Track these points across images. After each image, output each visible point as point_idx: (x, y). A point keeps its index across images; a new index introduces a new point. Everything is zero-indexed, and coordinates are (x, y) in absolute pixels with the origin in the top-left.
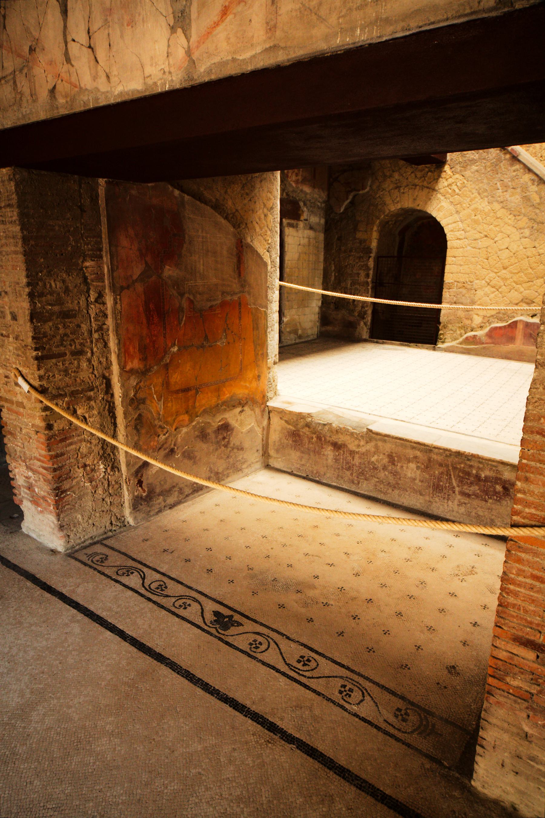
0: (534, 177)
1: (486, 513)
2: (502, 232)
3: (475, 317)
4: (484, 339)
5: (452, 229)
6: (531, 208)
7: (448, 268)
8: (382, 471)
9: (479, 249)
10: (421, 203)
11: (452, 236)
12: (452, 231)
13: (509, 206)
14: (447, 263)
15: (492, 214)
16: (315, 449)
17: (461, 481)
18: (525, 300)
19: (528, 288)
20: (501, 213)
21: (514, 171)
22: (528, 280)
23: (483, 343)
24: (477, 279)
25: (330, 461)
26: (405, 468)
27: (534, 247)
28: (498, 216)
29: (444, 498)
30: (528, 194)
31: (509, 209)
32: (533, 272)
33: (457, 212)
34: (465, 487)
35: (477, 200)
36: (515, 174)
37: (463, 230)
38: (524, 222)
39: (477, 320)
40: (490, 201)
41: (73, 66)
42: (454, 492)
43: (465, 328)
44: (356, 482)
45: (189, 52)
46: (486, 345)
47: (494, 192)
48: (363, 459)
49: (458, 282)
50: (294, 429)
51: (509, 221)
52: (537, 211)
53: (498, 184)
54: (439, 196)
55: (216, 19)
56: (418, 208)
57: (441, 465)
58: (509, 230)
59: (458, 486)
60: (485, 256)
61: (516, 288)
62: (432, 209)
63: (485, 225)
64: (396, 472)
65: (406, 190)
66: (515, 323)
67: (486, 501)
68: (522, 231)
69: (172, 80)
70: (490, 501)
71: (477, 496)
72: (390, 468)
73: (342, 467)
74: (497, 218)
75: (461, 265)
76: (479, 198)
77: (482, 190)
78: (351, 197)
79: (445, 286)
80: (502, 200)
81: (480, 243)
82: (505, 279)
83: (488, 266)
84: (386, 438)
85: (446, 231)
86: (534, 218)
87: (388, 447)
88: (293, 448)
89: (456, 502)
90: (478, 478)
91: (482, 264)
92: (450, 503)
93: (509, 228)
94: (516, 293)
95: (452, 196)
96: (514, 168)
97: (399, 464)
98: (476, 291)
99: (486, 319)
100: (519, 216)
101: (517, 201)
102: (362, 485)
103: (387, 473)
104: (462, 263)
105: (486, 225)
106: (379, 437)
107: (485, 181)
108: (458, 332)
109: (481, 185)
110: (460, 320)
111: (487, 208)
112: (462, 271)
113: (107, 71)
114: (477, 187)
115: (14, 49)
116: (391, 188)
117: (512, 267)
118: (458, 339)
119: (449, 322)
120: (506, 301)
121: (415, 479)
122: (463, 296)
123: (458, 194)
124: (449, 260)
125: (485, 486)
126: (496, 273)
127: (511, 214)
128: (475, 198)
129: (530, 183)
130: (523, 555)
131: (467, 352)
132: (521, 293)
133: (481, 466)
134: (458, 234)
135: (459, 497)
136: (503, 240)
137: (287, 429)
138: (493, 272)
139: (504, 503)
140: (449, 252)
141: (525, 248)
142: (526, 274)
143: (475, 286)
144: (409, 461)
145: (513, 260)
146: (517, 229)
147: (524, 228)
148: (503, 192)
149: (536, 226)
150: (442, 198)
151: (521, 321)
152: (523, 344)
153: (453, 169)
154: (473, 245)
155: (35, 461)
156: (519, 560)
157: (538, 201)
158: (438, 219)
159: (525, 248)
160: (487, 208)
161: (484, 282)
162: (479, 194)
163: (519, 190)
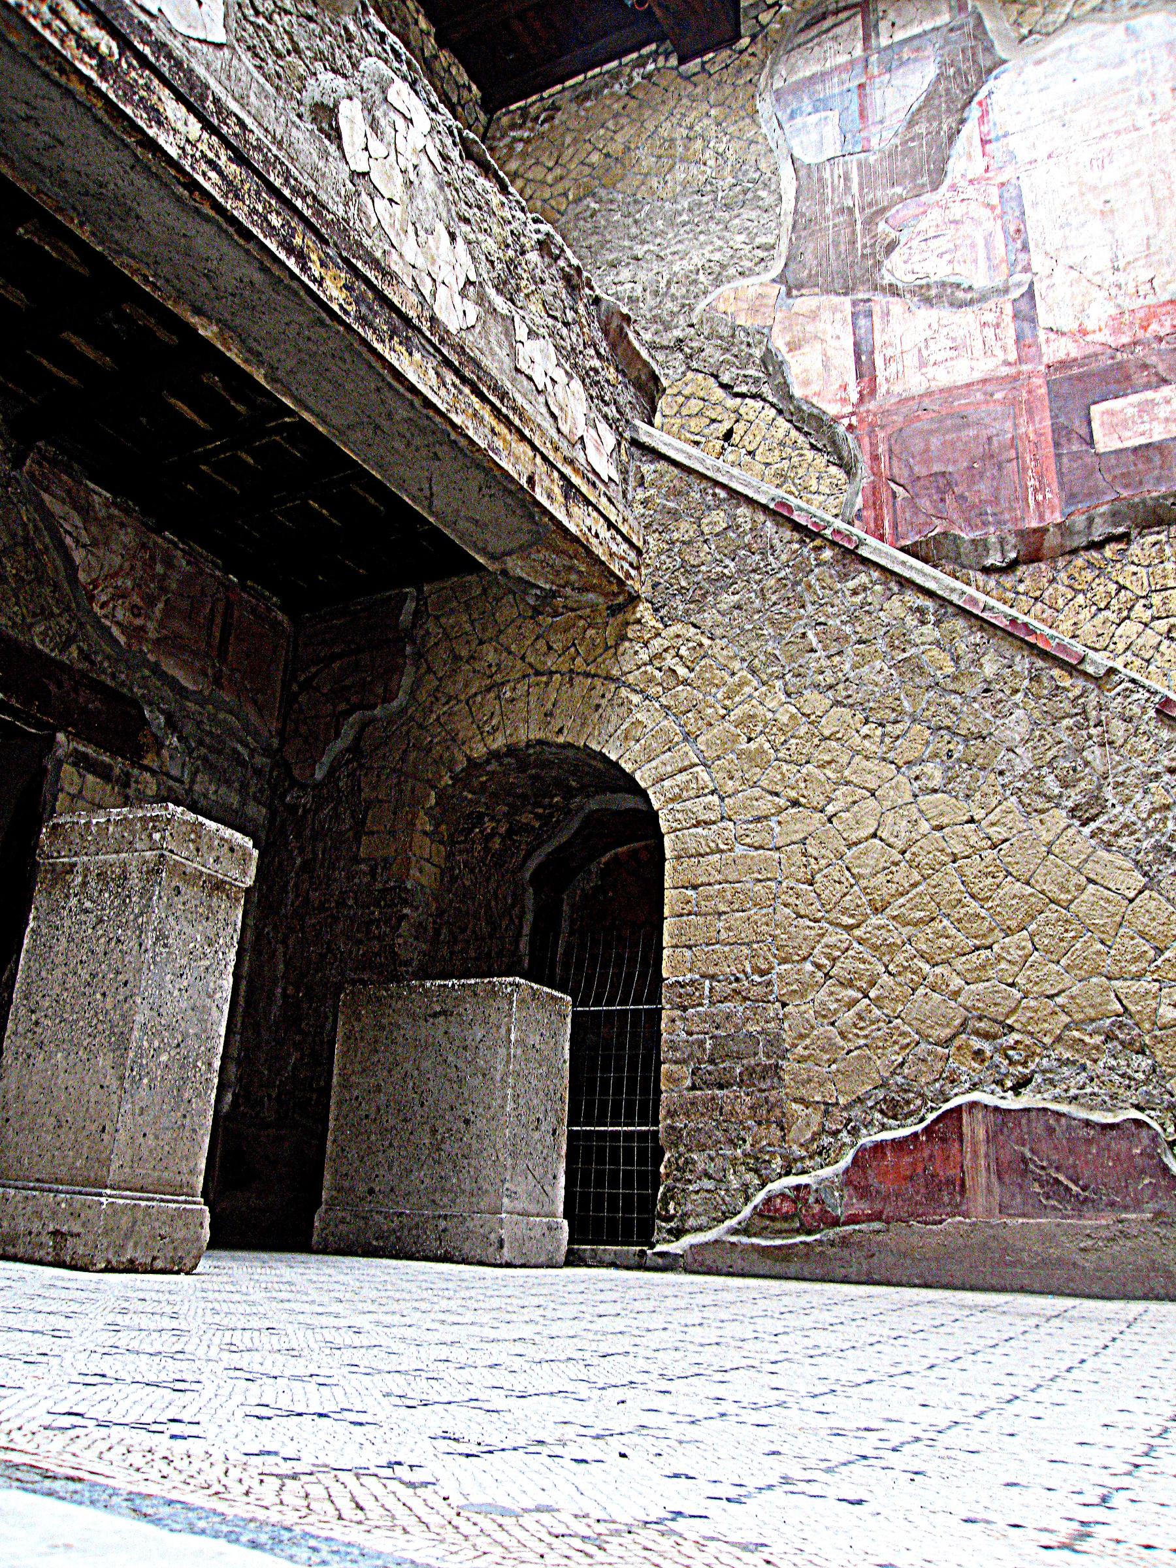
2: (847, 783)
4: (840, 1204)
5: (677, 790)
9: (778, 849)
11: (679, 816)
19: (978, 974)
21: (855, 593)
22: (972, 943)
23: (835, 1223)
24: (785, 961)
27: (971, 820)
28: (827, 733)
32: (983, 913)
35: (747, 690)
36: (858, 599)
37: (712, 793)
40: (792, 689)
46: (849, 1228)
47: (801, 661)
49: (713, 977)
51: (867, 743)
52: (956, 700)
53: (810, 634)
58: (871, 772)
61: (931, 979)
63: (785, 767)
68: (917, 770)
75: (720, 914)
76: (755, 683)
77: (763, 658)
78: (348, 733)
80: (831, 680)
81: (777, 829)
83: (818, 905)
86: (947, 722)
91: (793, 900)
96: (851, 584)
98: (784, 1005)
100: (896, 722)
101: (880, 679)
104: (722, 908)
105: (791, 766)
108: (735, 1184)
112: (723, 935)
117: (902, 900)
120: (904, 1034)
126: (849, 928)
127: (867, 722)
129: (911, 621)
132: (957, 993)
136: (856, 808)
138: (838, 925)
141: (940, 828)
142: (959, 921)
146: (898, 768)
148: (829, 657)
149: (959, 749)
150: (636, 699)
153: (663, 612)
159: (940, 828)
162: (753, 672)
163: (881, 645)
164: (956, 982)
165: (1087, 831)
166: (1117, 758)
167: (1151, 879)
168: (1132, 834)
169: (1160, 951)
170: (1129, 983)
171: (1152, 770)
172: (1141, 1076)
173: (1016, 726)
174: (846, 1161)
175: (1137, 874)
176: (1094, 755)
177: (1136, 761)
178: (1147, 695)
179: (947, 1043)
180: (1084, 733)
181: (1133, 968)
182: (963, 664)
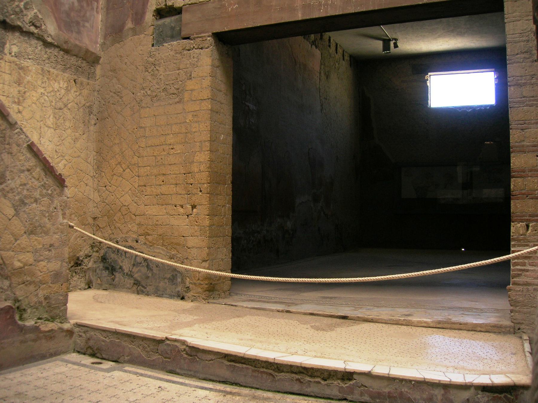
166: (12, 160)
167: (17, 212)
168: (13, 193)
169: (16, 240)
170: (5, 253)
171: (22, 168)
172: (5, 287)
175: (13, 209)
177: (18, 163)
178: (25, 137)
180: (3, 146)
181: (8, 247)
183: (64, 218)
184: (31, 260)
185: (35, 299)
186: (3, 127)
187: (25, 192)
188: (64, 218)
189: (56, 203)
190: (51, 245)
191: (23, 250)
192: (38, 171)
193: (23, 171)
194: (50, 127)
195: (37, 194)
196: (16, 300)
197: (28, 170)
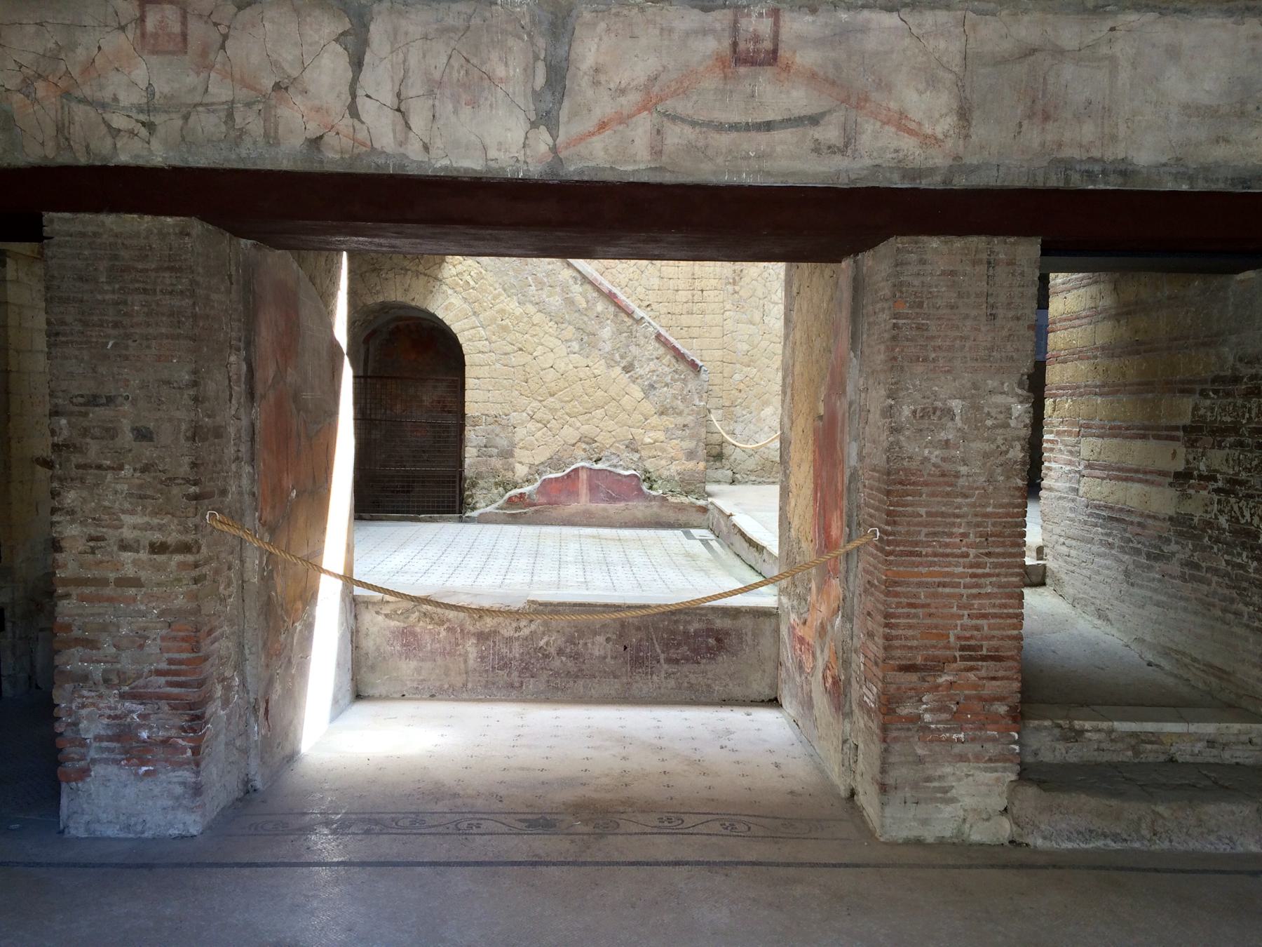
0: (575, 274)
1: (701, 679)
3: (518, 466)
6: (577, 315)
7: (469, 395)
8: (556, 657)
10: (417, 297)
12: (470, 340)
13: (548, 310)
14: (467, 387)
15: (525, 319)
16: (445, 649)
17: (667, 646)
18: (583, 439)
19: (587, 422)
20: (538, 318)
23: (535, 505)
25: (471, 662)
26: (589, 645)
29: (647, 673)
30: (570, 295)
31: (549, 314)
33: (475, 313)
34: (672, 651)
35: (502, 298)
38: (570, 332)
39: (521, 471)
41: (363, 123)
42: (658, 662)
43: (506, 485)
44: (517, 684)
45: (554, 149)
48: (527, 646)
50: (402, 625)
52: (586, 319)
53: (530, 278)
54: (444, 287)
55: (592, 129)
56: (413, 304)
57: (638, 629)
58: (552, 342)
59: (663, 652)
60: (522, 378)
62: (435, 307)
64: (577, 653)
65: (391, 275)
66: (576, 470)
67: (698, 663)
69: (528, 170)
70: (704, 661)
71: (687, 659)
72: (568, 650)
73: (493, 668)
74: (533, 325)
79: (468, 422)
82: (553, 410)
84: (561, 608)
85: (461, 340)
87: (560, 621)
88: (403, 657)
89: (663, 675)
90: (686, 633)
92: (655, 677)
93: (552, 339)
94: (571, 429)
95: (465, 290)
97: (581, 642)
99: (534, 468)
102: (527, 687)
103: (564, 659)
106: (549, 608)
107: (511, 273)
109: (505, 278)
110: (495, 473)
111: (519, 311)
113: (427, 141)
114: (500, 281)
115: (238, 76)
116: (364, 270)
118: (495, 502)
119: (479, 475)
121: (605, 658)
122: (497, 435)
123: (473, 288)
124: (469, 383)
125: (694, 643)
126: (541, 401)
128: (500, 295)
129: (571, 282)
130: (898, 589)
131: (514, 519)
132: (578, 429)
133: (689, 618)
134: (480, 345)
135: (666, 666)
137: (389, 628)
139: (720, 659)
140: (469, 372)
141: (576, 368)
143: (513, 421)
144: (595, 633)
145: (562, 383)
147: (570, 340)
150: (450, 292)
151: (583, 467)
152: (590, 501)
154: (505, 362)
155: (153, 678)
156: (897, 595)
157: (584, 305)
158: (448, 323)
159: (576, 368)
160: (519, 311)
161: (525, 414)
162: (505, 290)
163: (558, 289)
164: (578, 424)
165: (627, 375)
169: (646, 419)
173: (607, 332)
174: (537, 484)
176: (633, 348)
179: (573, 445)
182: (590, 304)
183: (700, 401)
184: (662, 438)
185: (668, 473)
186: (629, 324)
187: (655, 378)
188: (700, 401)
189: (692, 385)
190: (684, 426)
191: (654, 428)
192: (668, 358)
193: (652, 359)
194: (777, 303)
195: (668, 379)
196: (646, 471)
197: (657, 358)
